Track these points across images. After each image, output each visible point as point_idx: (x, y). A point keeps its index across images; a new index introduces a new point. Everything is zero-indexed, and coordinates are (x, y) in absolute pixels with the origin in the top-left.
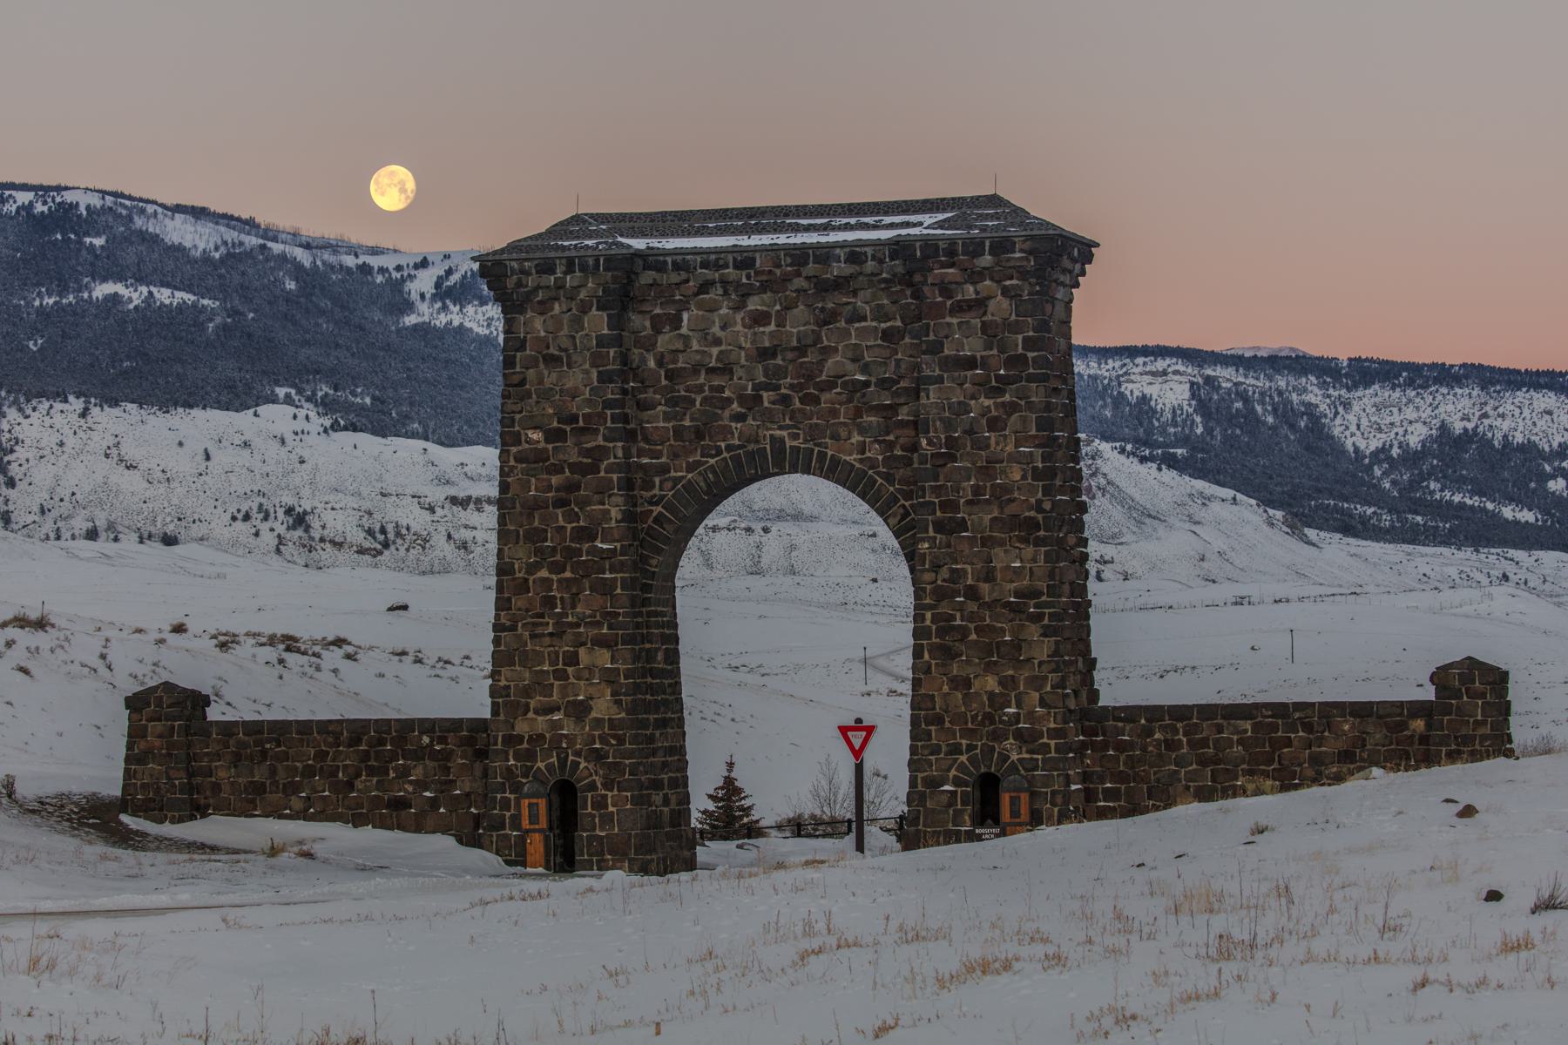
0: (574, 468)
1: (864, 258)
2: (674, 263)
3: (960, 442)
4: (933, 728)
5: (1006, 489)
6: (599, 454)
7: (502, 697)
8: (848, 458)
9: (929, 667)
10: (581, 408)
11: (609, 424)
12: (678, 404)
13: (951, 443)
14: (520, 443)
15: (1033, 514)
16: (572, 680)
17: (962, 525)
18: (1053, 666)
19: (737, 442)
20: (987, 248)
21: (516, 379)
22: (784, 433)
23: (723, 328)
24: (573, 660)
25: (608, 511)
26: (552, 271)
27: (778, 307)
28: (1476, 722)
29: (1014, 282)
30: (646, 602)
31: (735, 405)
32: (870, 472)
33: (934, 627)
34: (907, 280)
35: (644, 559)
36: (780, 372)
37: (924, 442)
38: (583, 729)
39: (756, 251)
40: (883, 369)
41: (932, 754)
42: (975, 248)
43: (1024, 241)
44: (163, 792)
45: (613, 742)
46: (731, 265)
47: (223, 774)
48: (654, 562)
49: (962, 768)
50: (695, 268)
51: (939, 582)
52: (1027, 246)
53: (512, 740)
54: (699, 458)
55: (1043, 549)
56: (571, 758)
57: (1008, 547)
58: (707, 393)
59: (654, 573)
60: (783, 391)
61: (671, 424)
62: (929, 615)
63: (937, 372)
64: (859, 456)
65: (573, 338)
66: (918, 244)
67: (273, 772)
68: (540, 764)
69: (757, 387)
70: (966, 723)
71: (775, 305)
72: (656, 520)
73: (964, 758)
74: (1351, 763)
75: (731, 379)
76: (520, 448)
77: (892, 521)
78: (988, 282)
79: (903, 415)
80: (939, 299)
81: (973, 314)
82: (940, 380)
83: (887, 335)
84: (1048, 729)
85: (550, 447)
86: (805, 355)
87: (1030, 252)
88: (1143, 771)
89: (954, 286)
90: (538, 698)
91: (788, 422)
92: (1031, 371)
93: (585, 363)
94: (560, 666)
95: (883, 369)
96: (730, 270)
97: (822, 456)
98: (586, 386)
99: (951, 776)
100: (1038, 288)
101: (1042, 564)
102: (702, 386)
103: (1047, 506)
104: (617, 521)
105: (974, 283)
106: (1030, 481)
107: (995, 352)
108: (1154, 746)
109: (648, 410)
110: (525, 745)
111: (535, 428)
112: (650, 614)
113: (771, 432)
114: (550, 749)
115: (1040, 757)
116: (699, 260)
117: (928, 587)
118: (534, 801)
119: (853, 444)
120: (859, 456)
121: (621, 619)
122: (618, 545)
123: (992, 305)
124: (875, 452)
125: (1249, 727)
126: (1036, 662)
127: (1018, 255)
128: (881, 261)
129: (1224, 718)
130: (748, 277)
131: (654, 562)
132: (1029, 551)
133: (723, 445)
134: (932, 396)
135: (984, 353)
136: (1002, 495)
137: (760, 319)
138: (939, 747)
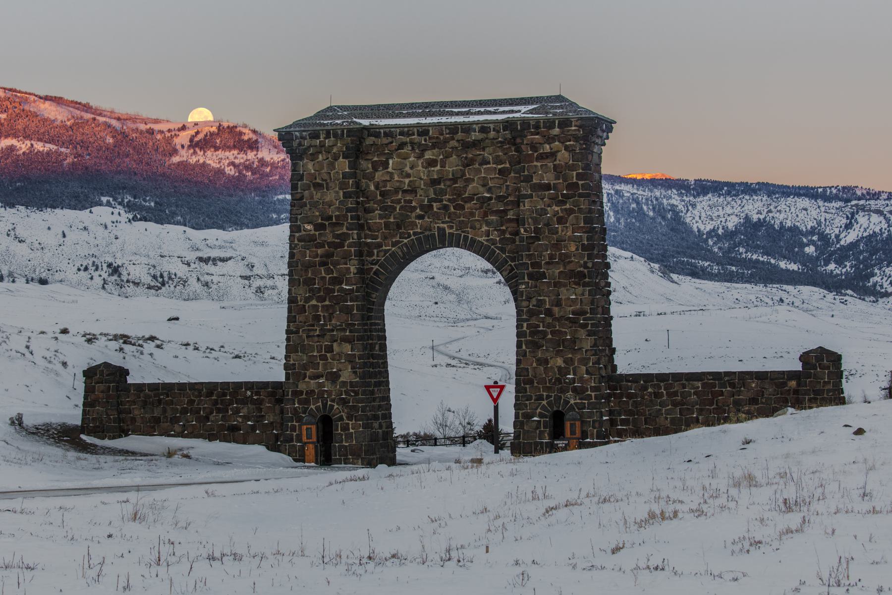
0: (331, 245)
1: (489, 130)
2: (385, 133)
3: (542, 230)
4: (528, 386)
5: (567, 256)
6: (344, 237)
7: (291, 370)
8: (480, 239)
9: (526, 353)
10: (333, 212)
11: (349, 221)
12: (387, 210)
13: (537, 230)
14: (300, 231)
15: (582, 269)
16: (330, 360)
17: (543, 275)
18: (593, 352)
19: (419, 230)
20: (557, 125)
21: (298, 196)
22: (445, 225)
23: (412, 168)
24: (330, 349)
25: (349, 268)
26: (318, 137)
27: (441, 157)
28: (825, 382)
29: (572, 143)
30: (369, 318)
31: (418, 210)
32: (492, 247)
33: (528, 331)
34: (513, 142)
35: (368, 295)
36: (443, 192)
37: (522, 230)
38: (336, 387)
39: (429, 126)
40: (499, 191)
41: (527, 400)
42: (550, 124)
43: (577, 121)
44: (104, 422)
45: (353, 394)
46: (416, 134)
47: (137, 412)
48: (374, 296)
49: (543, 408)
50: (396, 135)
51: (531, 307)
52: (578, 123)
53: (297, 393)
54: (398, 239)
55: (588, 288)
56: (329, 403)
57: (568, 287)
58: (403, 203)
59: (374, 302)
60: (445, 202)
61: (383, 221)
62: (525, 325)
63: (529, 192)
64: (486, 238)
65: (330, 173)
66: (519, 122)
67: (165, 411)
68: (313, 407)
69: (430, 200)
70: (546, 383)
71: (440, 156)
72: (375, 273)
73: (544, 402)
74: (756, 404)
75: (416, 196)
76: (301, 234)
77: (505, 273)
78: (557, 143)
79: (510, 215)
80: (530, 152)
81: (549, 160)
82: (531, 196)
83: (501, 172)
84: (591, 387)
85: (317, 233)
86: (456, 183)
87: (580, 127)
88: (642, 409)
89: (538, 145)
90: (311, 370)
91: (447, 219)
92: (581, 191)
93: (336, 187)
94: (323, 353)
95: (499, 191)
96: (415, 136)
97: (466, 238)
98: (336, 200)
100: (584, 146)
101: (587, 297)
102: (400, 200)
103: (590, 265)
104: (354, 274)
105: (549, 144)
106: (580, 251)
107: (561, 181)
108: (648, 396)
109: (370, 213)
110: (304, 396)
111: (309, 223)
112: (371, 324)
113: (438, 225)
114: (318, 398)
115: (586, 402)
116: (398, 131)
117: (525, 309)
118: (310, 426)
119: (483, 231)
120: (486, 238)
121: (356, 327)
122: (355, 287)
123: (559, 155)
124: (495, 236)
125: (700, 385)
126: (584, 350)
127: (573, 128)
128: (498, 132)
129: (686, 380)
130: (425, 140)
131: (374, 296)
132: (580, 289)
133: (411, 232)
134: (527, 205)
135: (555, 182)
136: (565, 259)
137: (431, 163)
138: (531, 396)
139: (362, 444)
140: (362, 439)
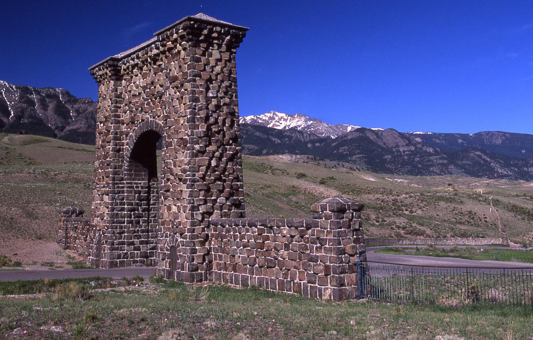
8: (160, 122)
15: (186, 137)
73: (168, 239)
115: (185, 240)
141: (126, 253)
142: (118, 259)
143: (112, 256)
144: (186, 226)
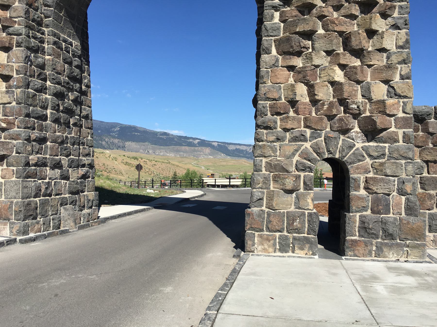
4: (278, 117)
49: (305, 155)
73: (307, 145)
99: (294, 162)
115: (387, 145)
121: (16, 26)
139: (12, 202)
140: (14, 194)
141: (49, 182)
142: (35, 197)
143: (26, 190)
144: (395, 112)
